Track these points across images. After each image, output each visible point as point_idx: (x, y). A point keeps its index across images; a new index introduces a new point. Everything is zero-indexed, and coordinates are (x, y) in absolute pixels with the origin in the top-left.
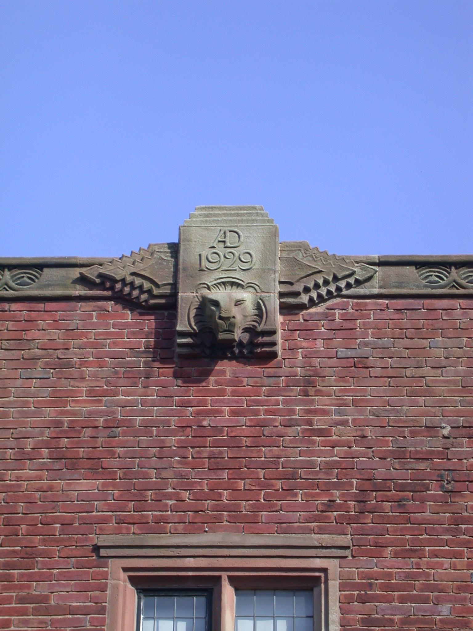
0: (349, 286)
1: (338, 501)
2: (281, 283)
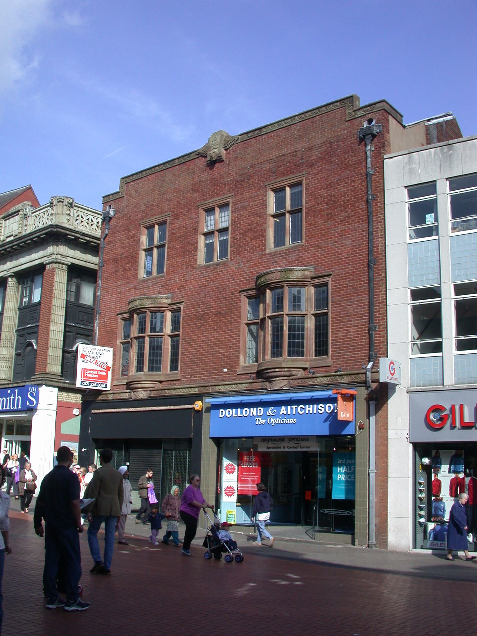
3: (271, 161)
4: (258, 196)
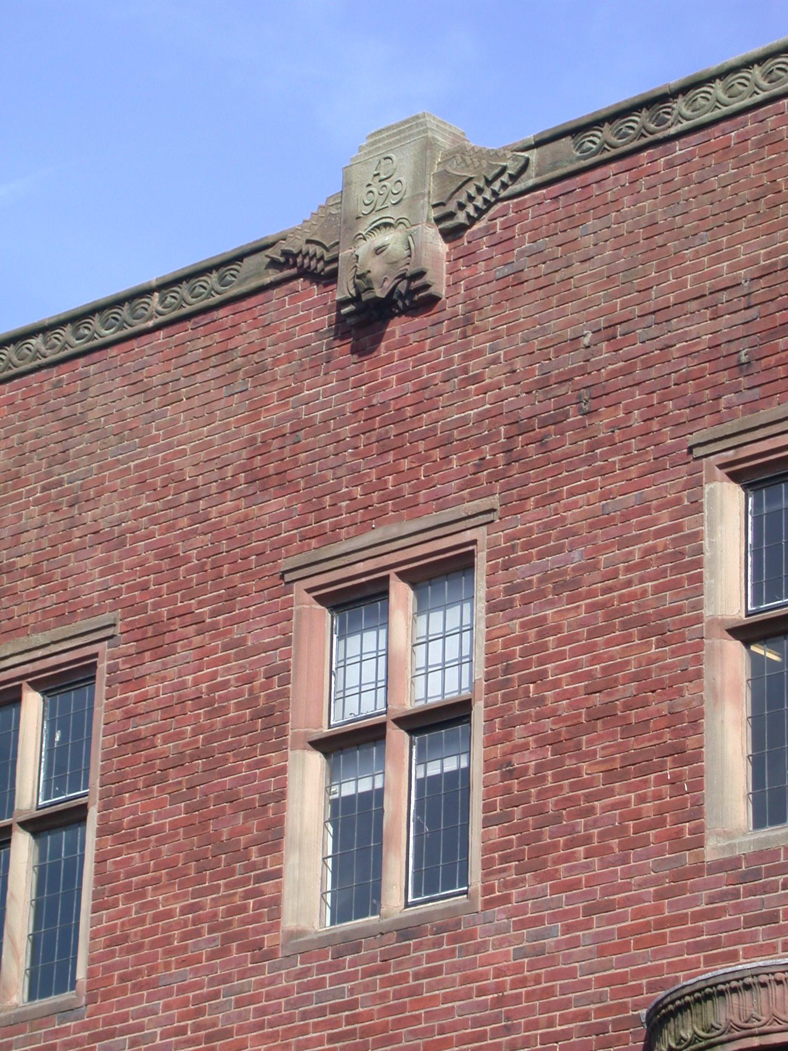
0: (504, 186)
1: (488, 457)
2: (434, 206)
3: (725, 296)
4: (647, 511)
